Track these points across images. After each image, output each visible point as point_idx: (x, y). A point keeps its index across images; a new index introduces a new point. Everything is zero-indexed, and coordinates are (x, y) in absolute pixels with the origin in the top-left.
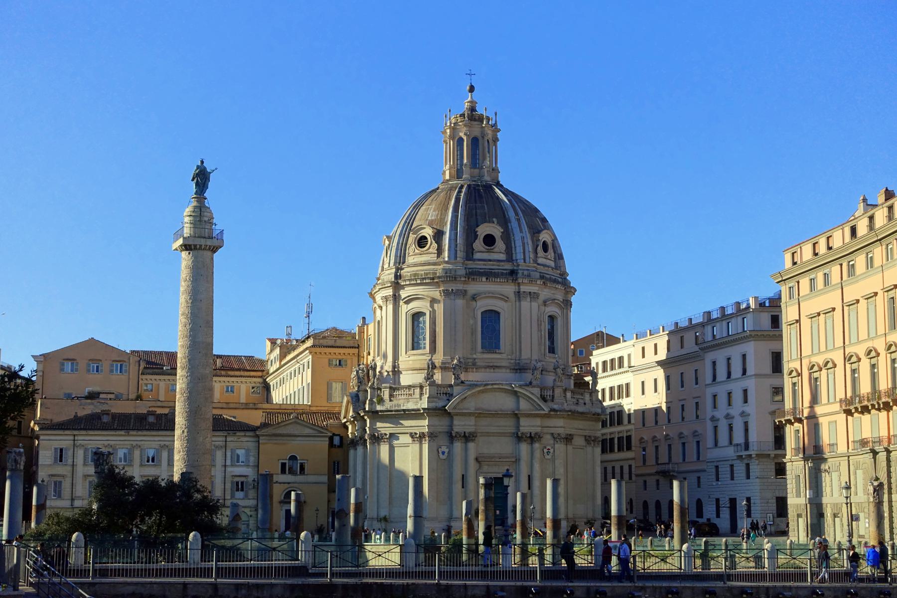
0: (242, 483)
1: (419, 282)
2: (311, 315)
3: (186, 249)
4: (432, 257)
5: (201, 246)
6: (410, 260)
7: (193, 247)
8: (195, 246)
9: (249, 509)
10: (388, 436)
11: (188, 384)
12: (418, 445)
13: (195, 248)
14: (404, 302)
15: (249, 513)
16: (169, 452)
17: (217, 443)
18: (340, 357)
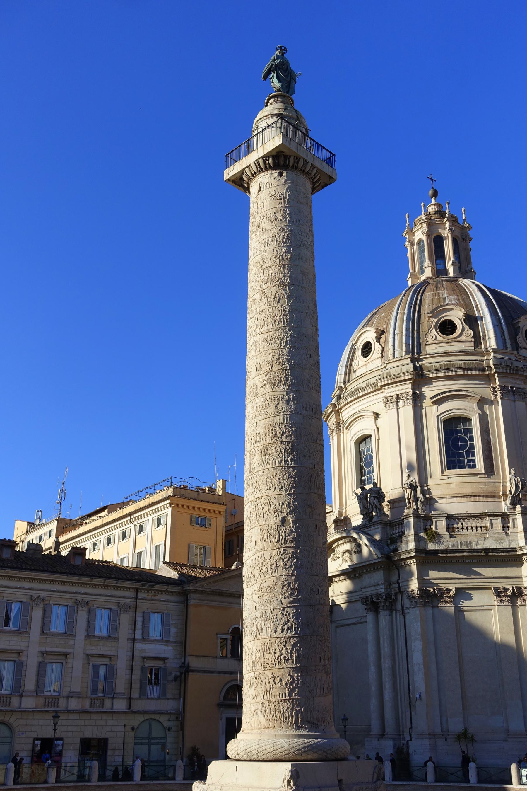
0: (158, 670)
1: (460, 373)
2: (63, 502)
3: (276, 166)
4: (470, 346)
5: (306, 162)
6: (430, 349)
7: (291, 162)
8: (297, 159)
9: (166, 717)
10: (453, 593)
11: (291, 415)
12: (510, 608)
13: (295, 168)
14: (433, 403)
15: (167, 724)
16: (44, 610)
17: (122, 601)
18: (203, 514)
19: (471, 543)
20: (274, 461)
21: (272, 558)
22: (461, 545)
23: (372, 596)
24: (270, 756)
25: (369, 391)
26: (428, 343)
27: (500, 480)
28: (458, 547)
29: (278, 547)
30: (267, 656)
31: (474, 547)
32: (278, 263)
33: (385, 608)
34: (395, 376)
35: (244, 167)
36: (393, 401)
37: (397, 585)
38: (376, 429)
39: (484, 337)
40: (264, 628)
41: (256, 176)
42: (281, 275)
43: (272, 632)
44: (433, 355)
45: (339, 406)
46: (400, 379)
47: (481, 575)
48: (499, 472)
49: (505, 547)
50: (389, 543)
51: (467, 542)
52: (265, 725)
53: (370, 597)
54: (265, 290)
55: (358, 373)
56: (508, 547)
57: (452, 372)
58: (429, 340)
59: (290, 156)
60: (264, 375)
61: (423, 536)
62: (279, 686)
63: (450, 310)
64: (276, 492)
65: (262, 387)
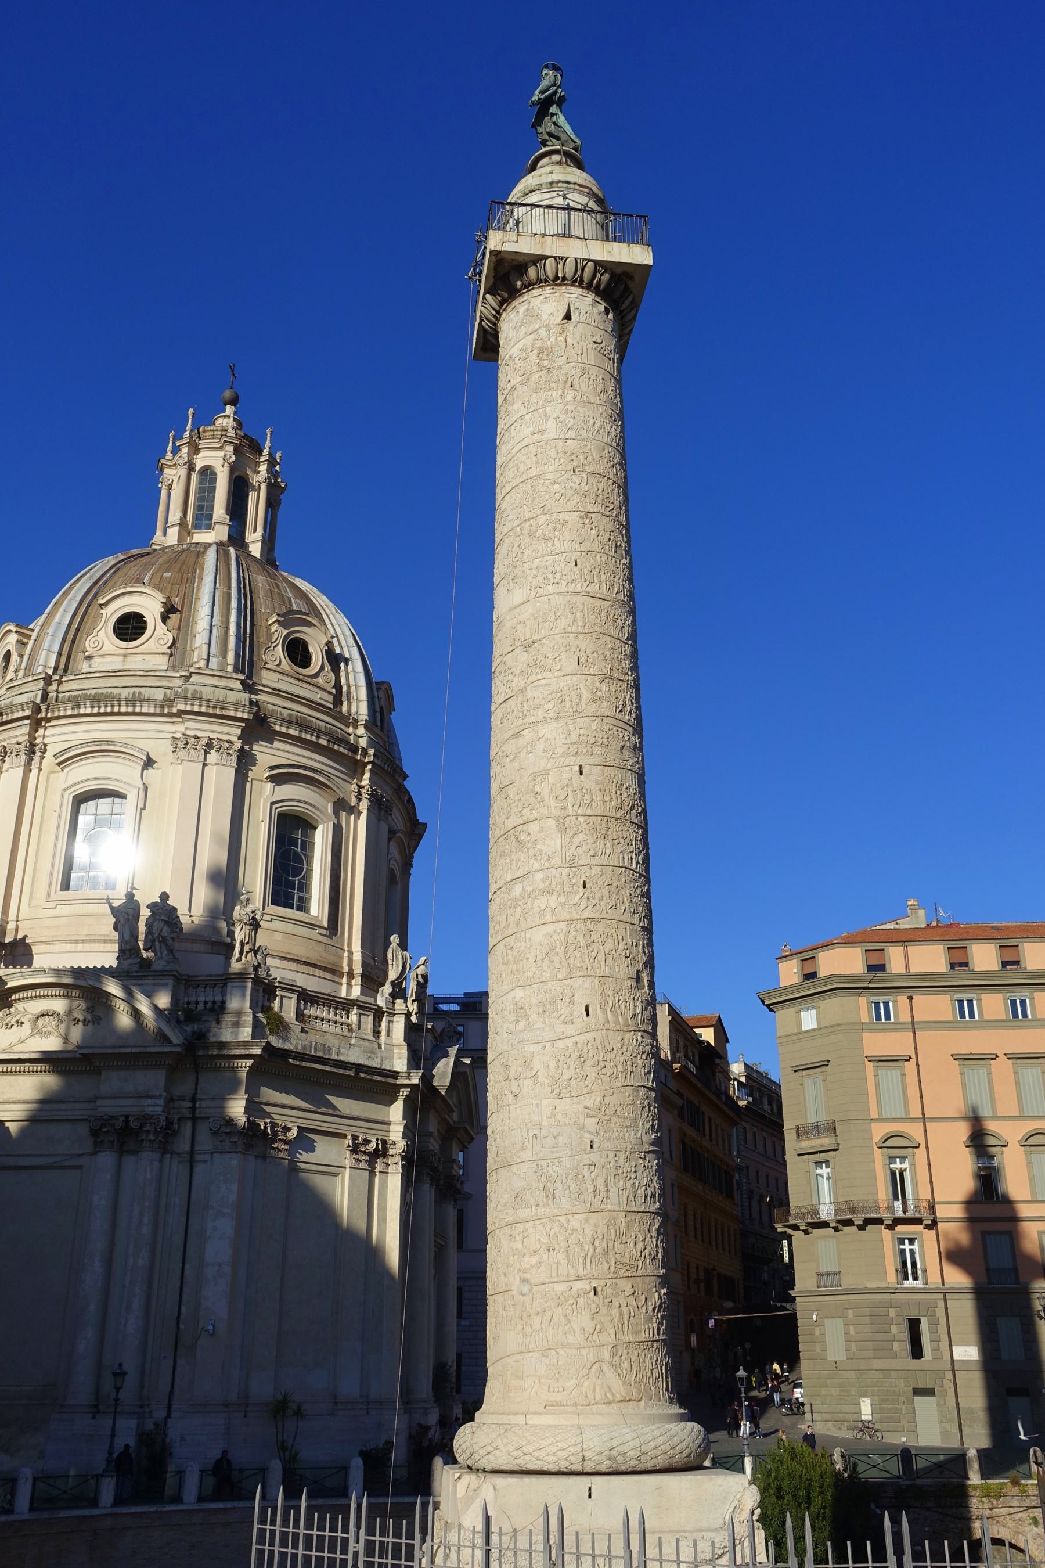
4: (327, 700)
19: (330, 1049)
20: (621, 856)
21: (624, 1048)
22: (316, 1049)
23: (127, 1117)
24: (660, 1462)
25: (145, 710)
26: (267, 666)
27: (343, 945)
28: (311, 1051)
29: (633, 1029)
30: (619, 1248)
31: (334, 1056)
32: (611, 476)
33: (156, 1145)
34: (219, 705)
35: (548, 253)
36: (198, 747)
37: (190, 1104)
38: (142, 787)
39: (349, 693)
40: (613, 1190)
41: (560, 285)
42: (617, 503)
43: (630, 1199)
44: (277, 692)
45: (47, 712)
46: (225, 713)
47: (335, 1108)
48: (343, 933)
49: (375, 1065)
50: (182, 1018)
51: (324, 1045)
52: (623, 1394)
53: (122, 1119)
54: (593, 515)
55: (99, 664)
56: (379, 1067)
57: (312, 735)
58: (270, 662)
59: (631, 292)
60: (596, 678)
61: (262, 1019)
62: (644, 1312)
63: (310, 624)
64: (624, 918)
65: (594, 701)
